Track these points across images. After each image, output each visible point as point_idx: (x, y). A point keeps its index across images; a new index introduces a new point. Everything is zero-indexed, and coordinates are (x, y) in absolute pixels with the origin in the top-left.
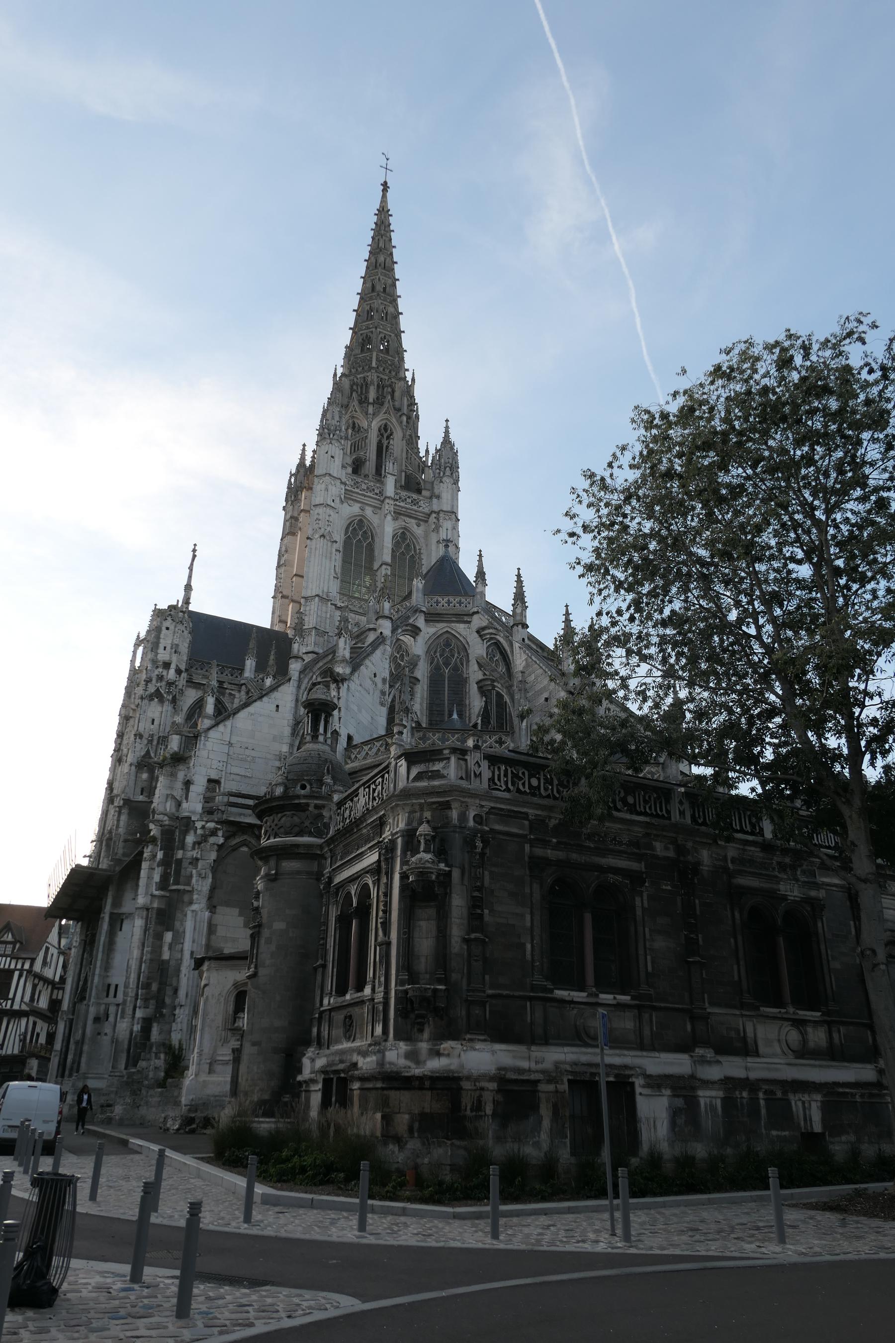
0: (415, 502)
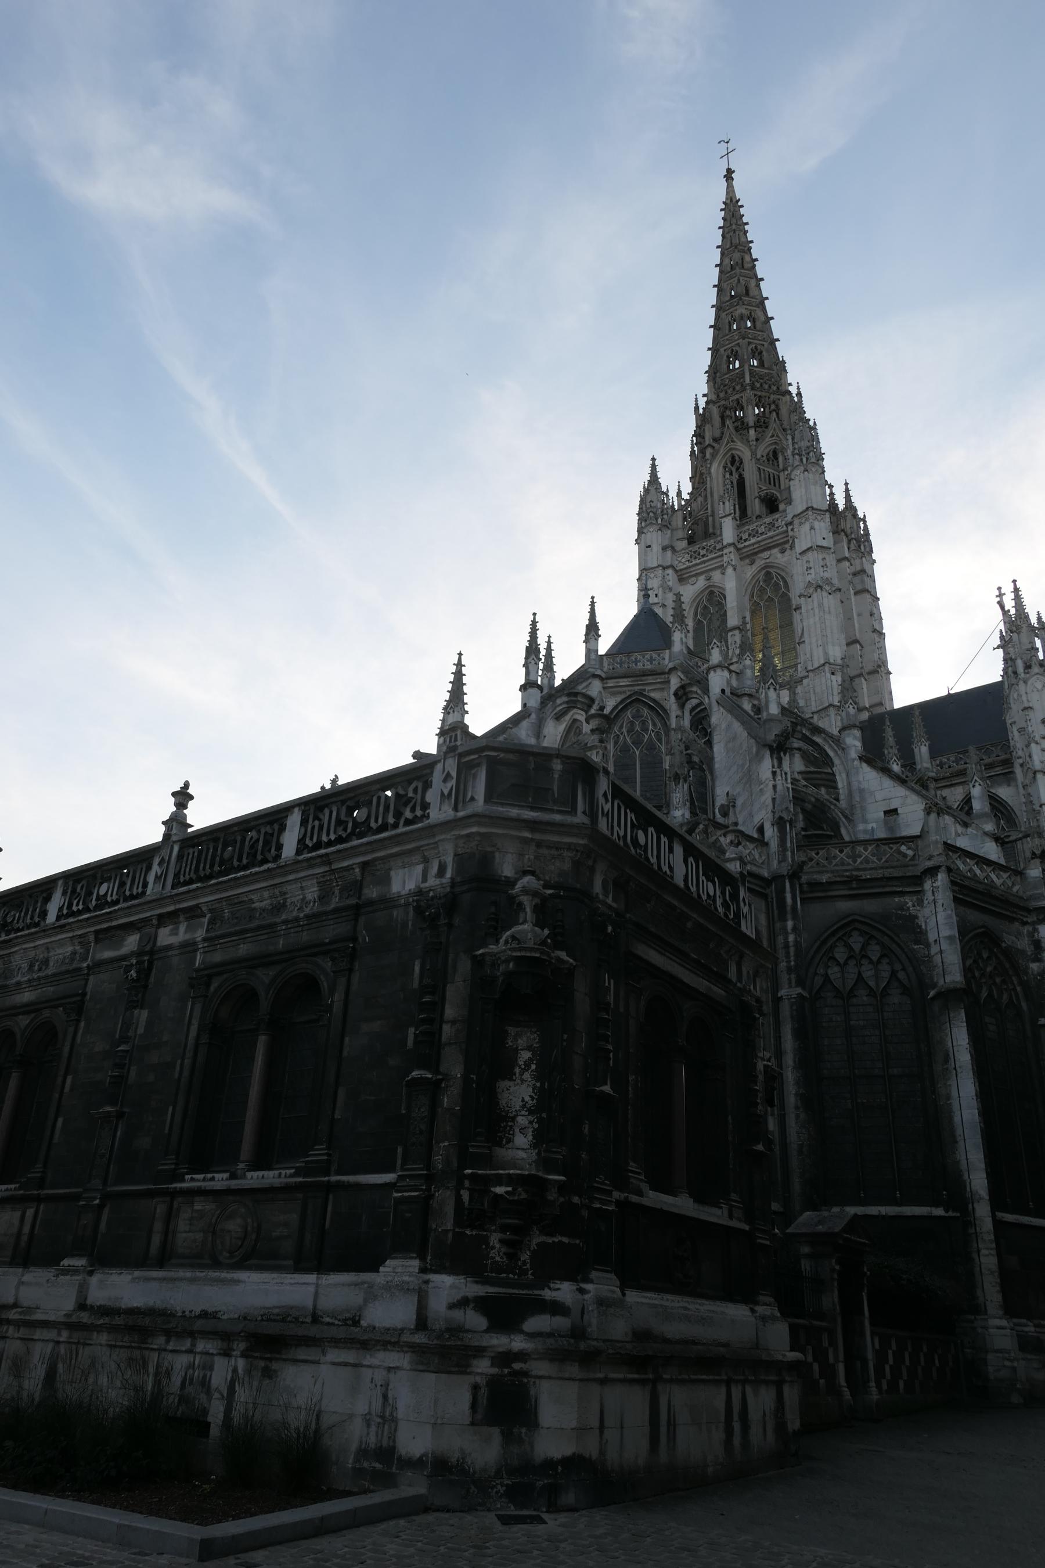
0: (772, 525)
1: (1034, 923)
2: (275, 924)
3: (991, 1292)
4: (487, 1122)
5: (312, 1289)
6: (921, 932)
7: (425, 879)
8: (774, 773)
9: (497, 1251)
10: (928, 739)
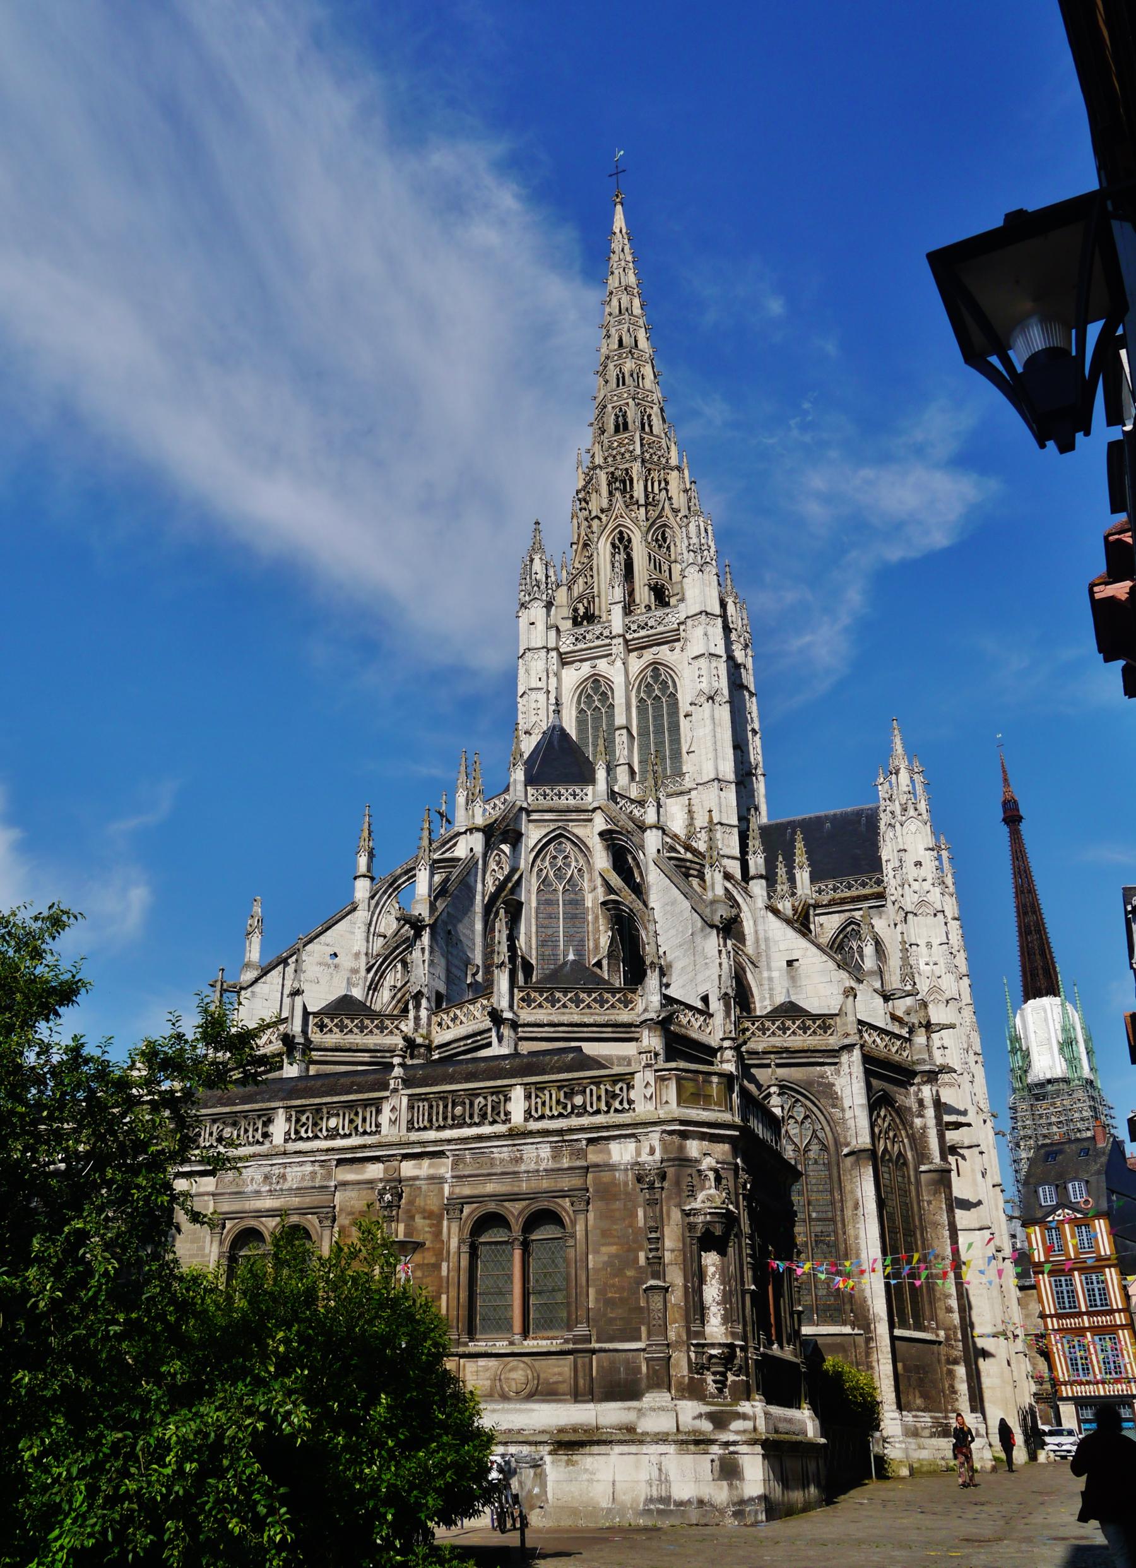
1: (919, 1084)
2: (518, 1173)
3: (886, 1393)
4: (697, 1310)
5: (594, 1413)
6: (837, 1098)
7: (638, 1154)
8: (720, 951)
9: (712, 1388)
10: (809, 865)
